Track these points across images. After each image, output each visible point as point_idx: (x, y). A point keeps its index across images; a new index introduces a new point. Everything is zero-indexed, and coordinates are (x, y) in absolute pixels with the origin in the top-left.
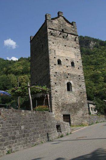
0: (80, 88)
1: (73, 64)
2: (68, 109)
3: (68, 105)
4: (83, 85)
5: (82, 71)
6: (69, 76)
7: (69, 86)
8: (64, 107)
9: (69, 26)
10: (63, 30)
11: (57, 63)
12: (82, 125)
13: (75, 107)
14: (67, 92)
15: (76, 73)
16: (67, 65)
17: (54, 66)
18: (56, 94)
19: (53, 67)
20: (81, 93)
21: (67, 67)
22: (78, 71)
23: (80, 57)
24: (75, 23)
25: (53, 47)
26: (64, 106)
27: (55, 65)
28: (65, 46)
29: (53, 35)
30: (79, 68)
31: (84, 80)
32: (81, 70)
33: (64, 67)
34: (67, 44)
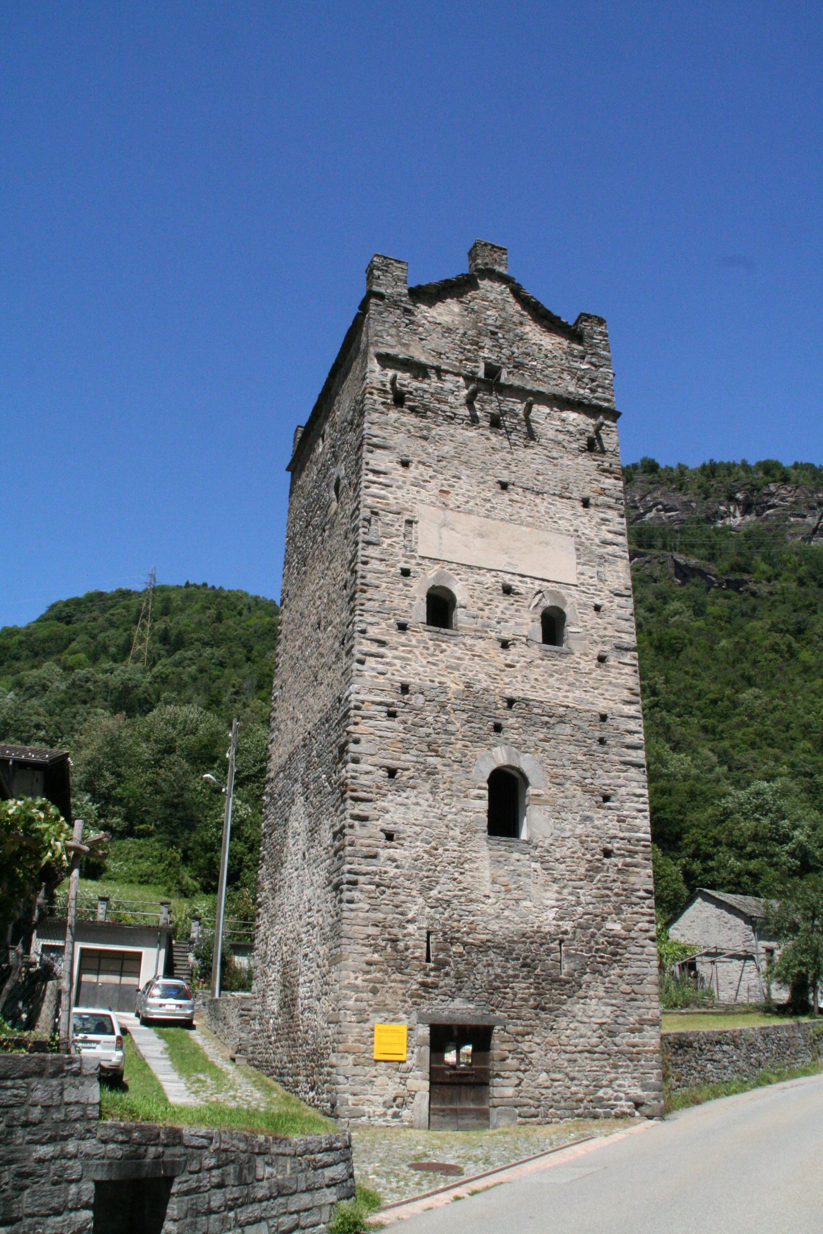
0: (598, 816)
1: (553, 626)
2: (481, 977)
3: (483, 947)
4: (633, 789)
5: (633, 681)
6: (511, 721)
7: (506, 801)
8: (445, 963)
9: (549, 342)
10: (492, 371)
11: (419, 612)
12: (592, 1111)
13: (542, 972)
14: (483, 849)
15: (574, 697)
16: (505, 635)
17: (395, 637)
18: (384, 853)
19: (382, 643)
20: (607, 853)
21: (505, 645)
22: (603, 684)
23: (620, 575)
24: (601, 322)
25: (393, 497)
26: (446, 955)
27: (402, 627)
28: (504, 486)
29: (412, 409)
30: (602, 659)
31: (639, 756)
32: (625, 675)
33: (480, 645)
34: (525, 474)
